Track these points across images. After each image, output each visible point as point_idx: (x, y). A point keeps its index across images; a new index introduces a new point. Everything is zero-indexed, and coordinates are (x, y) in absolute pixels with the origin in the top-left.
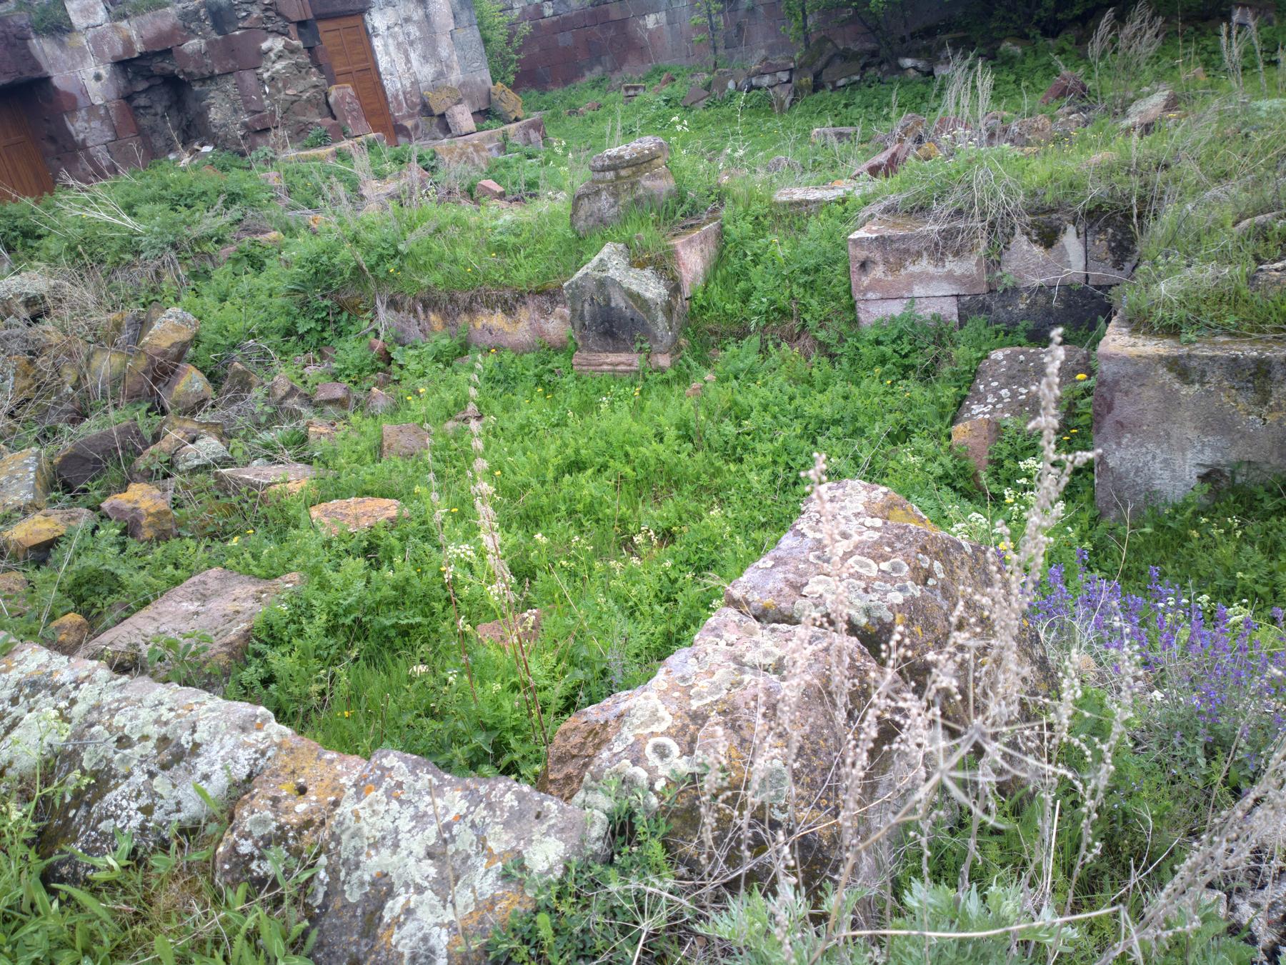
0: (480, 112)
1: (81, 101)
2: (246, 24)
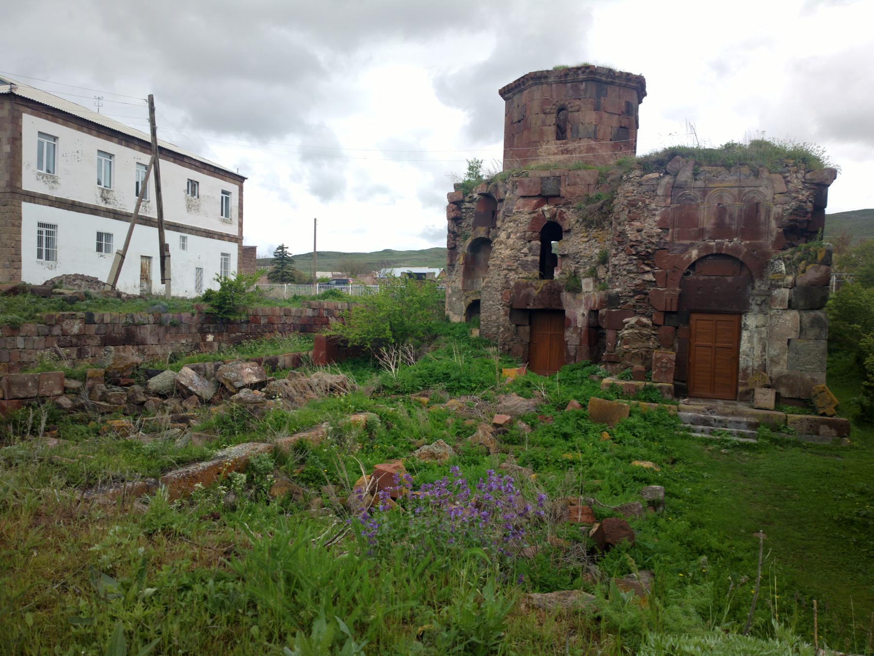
0: (799, 399)
1: (573, 323)
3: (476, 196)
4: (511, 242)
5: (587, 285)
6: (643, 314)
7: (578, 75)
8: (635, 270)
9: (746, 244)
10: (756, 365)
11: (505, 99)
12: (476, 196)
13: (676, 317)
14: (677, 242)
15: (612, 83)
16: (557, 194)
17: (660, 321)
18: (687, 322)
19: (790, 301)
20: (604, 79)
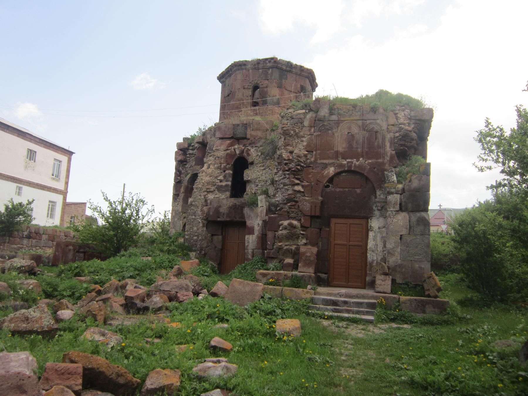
2: (280, 213)
3: (197, 145)
4: (212, 172)
5: (261, 201)
6: (294, 218)
7: (266, 63)
8: (288, 183)
9: (369, 163)
10: (379, 259)
11: (221, 82)
12: (197, 145)
13: (320, 220)
14: (319, 161)
15: (290, 71)
16: (244, 136)
17: (307, 224)
18: (328, 225)
19: (400, 204)
20: (284, 68)
